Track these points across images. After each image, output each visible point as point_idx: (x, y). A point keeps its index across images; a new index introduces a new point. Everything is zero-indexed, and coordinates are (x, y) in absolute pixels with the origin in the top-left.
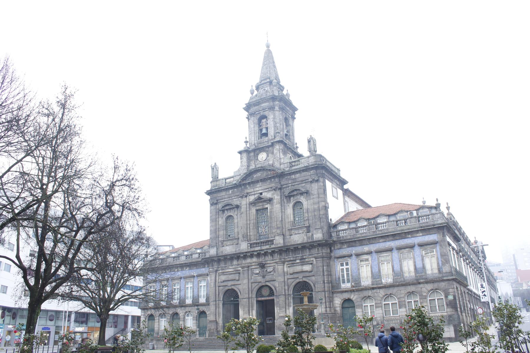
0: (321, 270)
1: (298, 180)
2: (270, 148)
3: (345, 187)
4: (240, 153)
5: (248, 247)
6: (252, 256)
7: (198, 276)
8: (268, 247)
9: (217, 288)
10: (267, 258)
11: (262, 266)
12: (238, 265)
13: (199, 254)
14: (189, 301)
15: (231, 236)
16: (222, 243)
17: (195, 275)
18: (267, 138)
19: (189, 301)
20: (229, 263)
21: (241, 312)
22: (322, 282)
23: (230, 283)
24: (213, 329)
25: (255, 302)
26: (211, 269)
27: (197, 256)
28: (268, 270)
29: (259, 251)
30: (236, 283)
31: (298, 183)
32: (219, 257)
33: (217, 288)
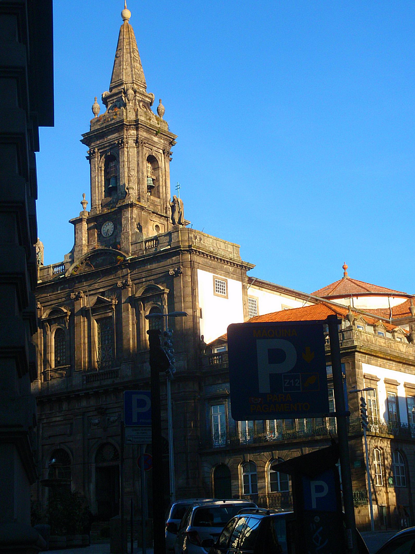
6: (87, 396)
8: (109, 382)
25: (93, 470)
28: (112, 419)
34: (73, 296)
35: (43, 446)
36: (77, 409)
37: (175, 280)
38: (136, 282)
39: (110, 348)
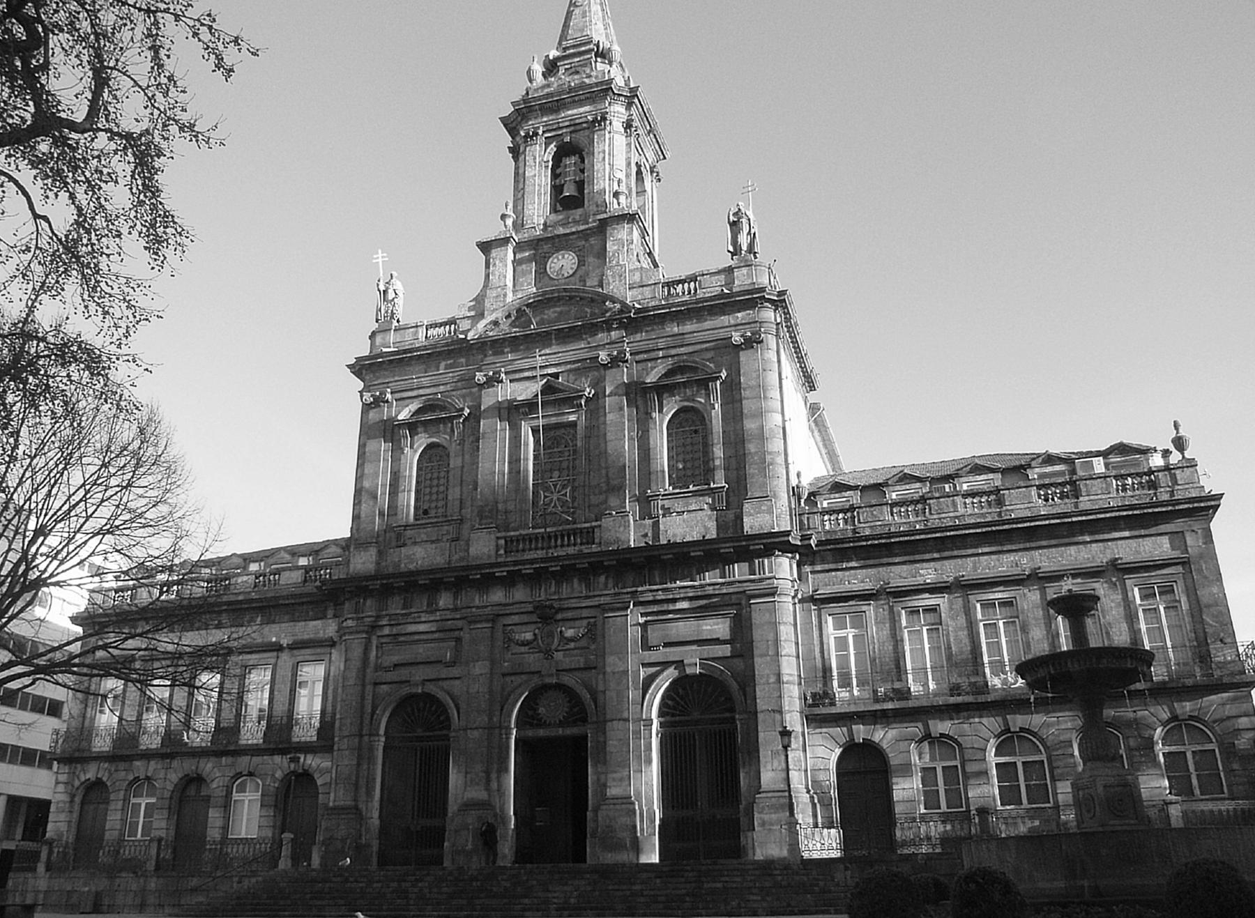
0: (771, 636)
1: (689, 339)
2: (593, 241)
3: (813, 397)
4: (485, 247)
5: (498, 548)
6: (510, 580)
7: (296, 646)
9: (369, 688)
10: (565, 590)
11: (546, 615)
12: (456, 609)
13: (307, 569)
14: (252, 733)
15: (432, 513)
16: (399, 536)
17: (284, 642)
18: (580, 211)
19: (252, 733)
20: (421, 602)
21: (455, 778)
22: (772, 680)
23: (419, 674)
24: (343, 840)
26: (350, 623)
27: (297, 576)
29: (543, 560)
30: (445, 673)
31: (691, 349)
32: (388, 576)
33: (369, 688)
34: (480, 377)
35: (376, 684)
36: (478, 607)
37: (744, 356)
38: (638, 358)
39: (564, 487)
